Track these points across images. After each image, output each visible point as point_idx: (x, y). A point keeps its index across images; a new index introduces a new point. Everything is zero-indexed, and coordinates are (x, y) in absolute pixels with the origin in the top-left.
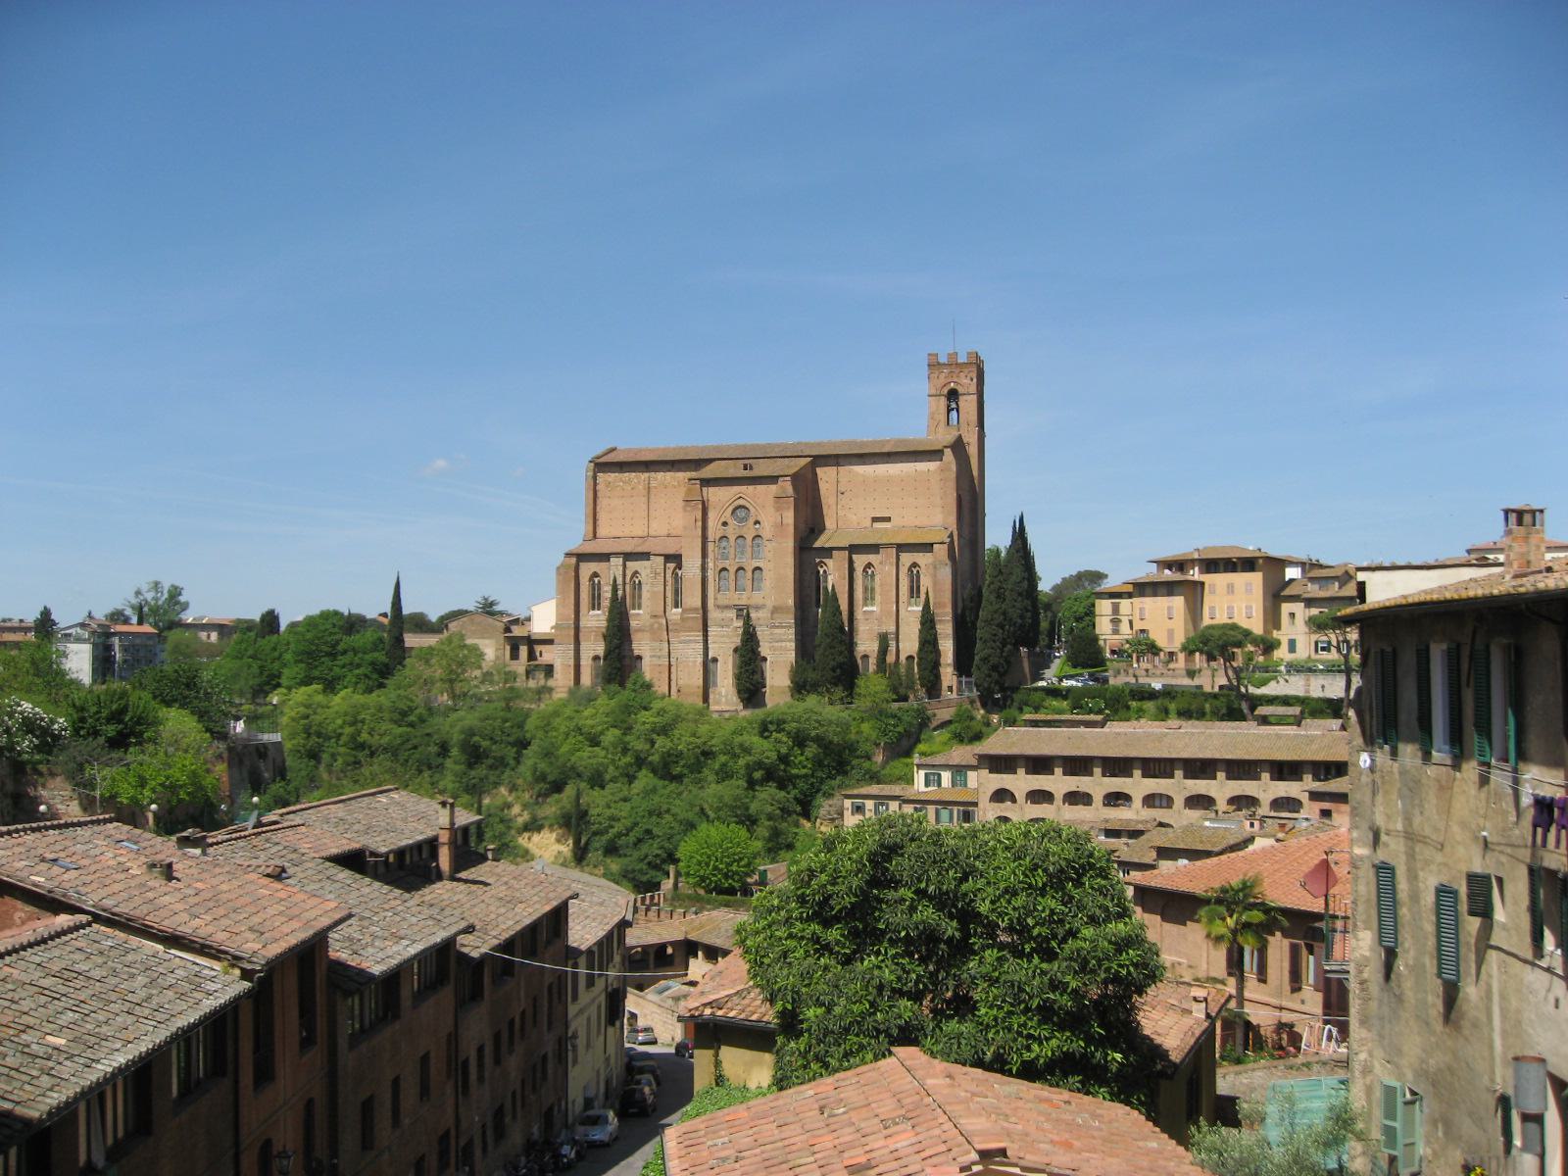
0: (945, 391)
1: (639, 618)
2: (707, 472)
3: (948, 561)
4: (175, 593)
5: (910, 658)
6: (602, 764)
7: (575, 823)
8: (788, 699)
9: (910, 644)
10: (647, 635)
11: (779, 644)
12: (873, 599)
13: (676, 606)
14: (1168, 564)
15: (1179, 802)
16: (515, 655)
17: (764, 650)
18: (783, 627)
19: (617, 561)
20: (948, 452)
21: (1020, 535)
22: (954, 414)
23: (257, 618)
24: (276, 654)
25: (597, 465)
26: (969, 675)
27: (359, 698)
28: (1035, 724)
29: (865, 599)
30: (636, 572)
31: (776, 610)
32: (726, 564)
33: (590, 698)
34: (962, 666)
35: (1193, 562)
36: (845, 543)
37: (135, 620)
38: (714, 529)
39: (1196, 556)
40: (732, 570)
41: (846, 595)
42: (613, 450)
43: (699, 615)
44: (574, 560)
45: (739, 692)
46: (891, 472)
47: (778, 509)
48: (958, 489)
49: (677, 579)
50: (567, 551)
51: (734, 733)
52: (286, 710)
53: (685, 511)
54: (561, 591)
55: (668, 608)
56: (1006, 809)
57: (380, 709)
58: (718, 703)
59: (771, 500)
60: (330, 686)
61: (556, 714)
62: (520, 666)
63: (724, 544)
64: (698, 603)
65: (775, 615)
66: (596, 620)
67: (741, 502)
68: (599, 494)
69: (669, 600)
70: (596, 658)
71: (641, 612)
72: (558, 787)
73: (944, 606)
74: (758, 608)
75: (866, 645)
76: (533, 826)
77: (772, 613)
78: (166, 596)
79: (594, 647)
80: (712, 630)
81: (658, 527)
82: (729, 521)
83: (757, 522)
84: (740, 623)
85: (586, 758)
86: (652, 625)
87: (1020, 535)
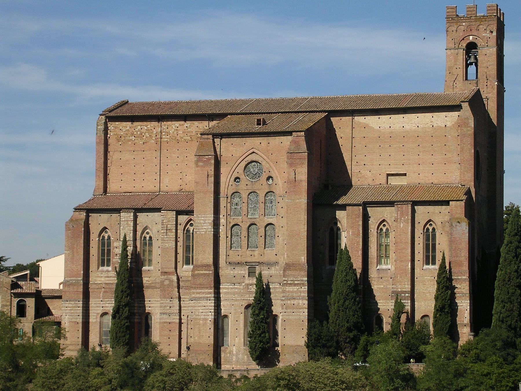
0: (464, 45)
3: (466, 220)
10: (157, 292)
11: (292, 302)
12: (387, 257)
13: (188, 263)
16: (21, 311)
17: (276, 309)
18: (295, 285)
19: (127, 217)
20: (466, 106)
22: (472, 69)
30: (146, 228)
31: (288, 267)
32: (238, 220)
36: (360, 200)
40: (245, 226)
41: (360, 252)
42: (125, 103)
43: (211, 272)
44: (83, 214)
46: (407, 127)
47: (291, 165)
48: (476, 145)
49: (188, 236)
50: (76, 205)
53: (197, 166)
54: (71, 248)
55: (179, 265)
58: (229, 362)
59: (283, 157)
63: (236, 200)
64: (210, 259)
65: (288, 272)
67: (253, 157)
68: (110, 148)
71: (152, 268)
73: (460, 265)
74: (269, 265)
77: (284, 271)
80: (224, 288)
82: (242, 177)
86: (162, 282)
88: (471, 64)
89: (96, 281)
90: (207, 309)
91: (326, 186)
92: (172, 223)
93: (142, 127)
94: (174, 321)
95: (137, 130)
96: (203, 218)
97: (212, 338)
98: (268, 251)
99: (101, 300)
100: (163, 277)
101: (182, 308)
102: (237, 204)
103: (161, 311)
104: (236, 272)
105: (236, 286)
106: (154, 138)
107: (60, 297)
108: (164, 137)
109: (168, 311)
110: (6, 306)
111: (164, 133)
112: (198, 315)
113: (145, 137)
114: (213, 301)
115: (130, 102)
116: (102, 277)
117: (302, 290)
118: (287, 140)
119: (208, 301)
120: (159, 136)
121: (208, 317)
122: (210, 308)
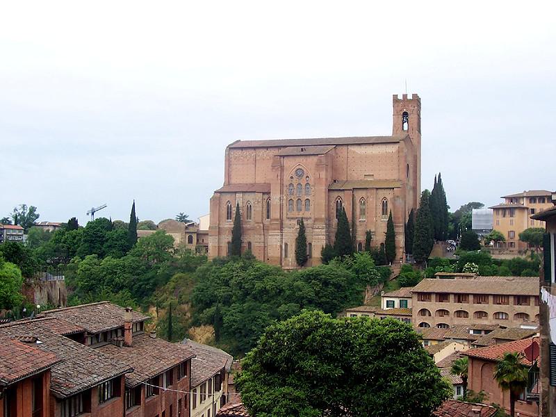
1: (248, 224)
2: (283, 151)
4: (33, 210)
5: (382, 244)
6: (230, 295)
7: (216, 321)
8: (320, 264)
9: (379, 238)
14: (511, 199)
15: (511, 316)
16: (190, 241)
17: (309, 239)
21: (438, 185)
22: (406, 125)
23: (67, 222)
24: (75, 241)
25: (230, 148)
26: (411, 253)
27: (115, 261)
28: (441, 277)
29: (361, 214)
33: (223, 262)
34: (408, 249)
35: (523, 197)
37: (13, 223)
38: (286, 182)
39: (525, 195)
40: (295, 200)
41: (351, 213)
45: (297, 260)
49: (268, 205)
51: (294, 280)
52: (80, 266)
56: (426, 319)
57: (124, 267)
60: (101, 256)
61: (208, 270)
62: (193, 247)
63: (291, 188)
66: (229, 225)
67: (300, 167)
69: (265, 216)
70: (229, 243)
72: (208, 305)
75: (361, 238)
76: (197, 323)
78: (28, 211)
79: (227, 238)
80: (285, 230)
81: (260, 180)
83: (307, 177)
84: (298, 227)
85: (221, 292)
87: (438, 185)
91: (335, 181)
98: (306, 212)
107: (207, 234)
118: (315, 159)
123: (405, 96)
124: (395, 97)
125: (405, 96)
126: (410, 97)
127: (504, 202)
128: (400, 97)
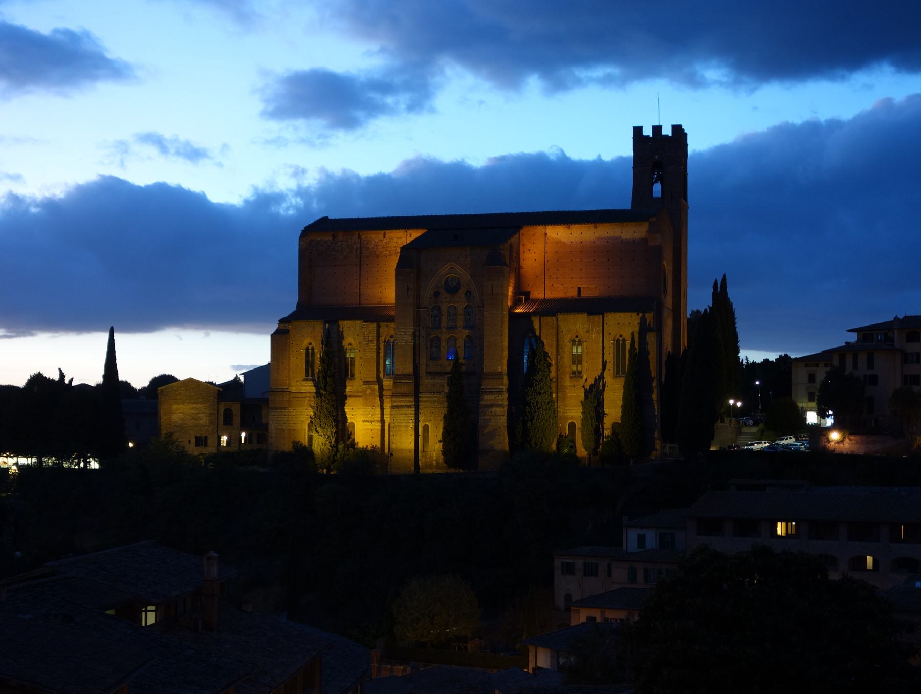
88: (656, 182)
89: (301, 389)
90: (409, 417)
92: (374, 335)
93: (343, 243)
94: (376, 428)
95: (338, 245)
96: (403, 330)
97: (413, 444)
99: (306, 408)
100: (365, 386)
101: (385, 416)
102: (436, 317)
103: (364, 419)
104: (436, 381)
105: (435, 395)
106: (354, 254)
108: (364, 252)
109: (370, 419)
110: (214, 414)
111: (363, 249)
112: (400, 423)
113: (345, 252)
114: (414, 409)
115: (330, 218)
116: (306, 386)
117: (499, 398)
119: (410, 409)
120: (359, 252)
121: (408, 424)
122: (411, 416)
123: (657, 129)
124: (638, 131)
125: (657, 129)
126: (667, 131)
127: (853, 338)
128: (648, 132)
